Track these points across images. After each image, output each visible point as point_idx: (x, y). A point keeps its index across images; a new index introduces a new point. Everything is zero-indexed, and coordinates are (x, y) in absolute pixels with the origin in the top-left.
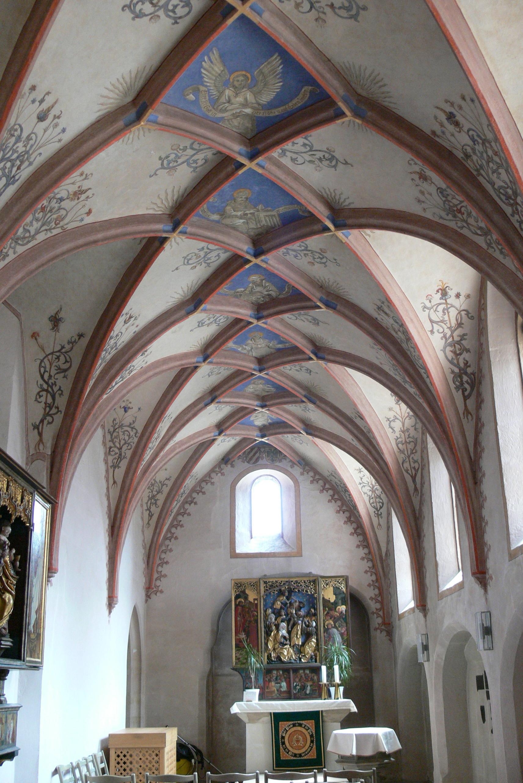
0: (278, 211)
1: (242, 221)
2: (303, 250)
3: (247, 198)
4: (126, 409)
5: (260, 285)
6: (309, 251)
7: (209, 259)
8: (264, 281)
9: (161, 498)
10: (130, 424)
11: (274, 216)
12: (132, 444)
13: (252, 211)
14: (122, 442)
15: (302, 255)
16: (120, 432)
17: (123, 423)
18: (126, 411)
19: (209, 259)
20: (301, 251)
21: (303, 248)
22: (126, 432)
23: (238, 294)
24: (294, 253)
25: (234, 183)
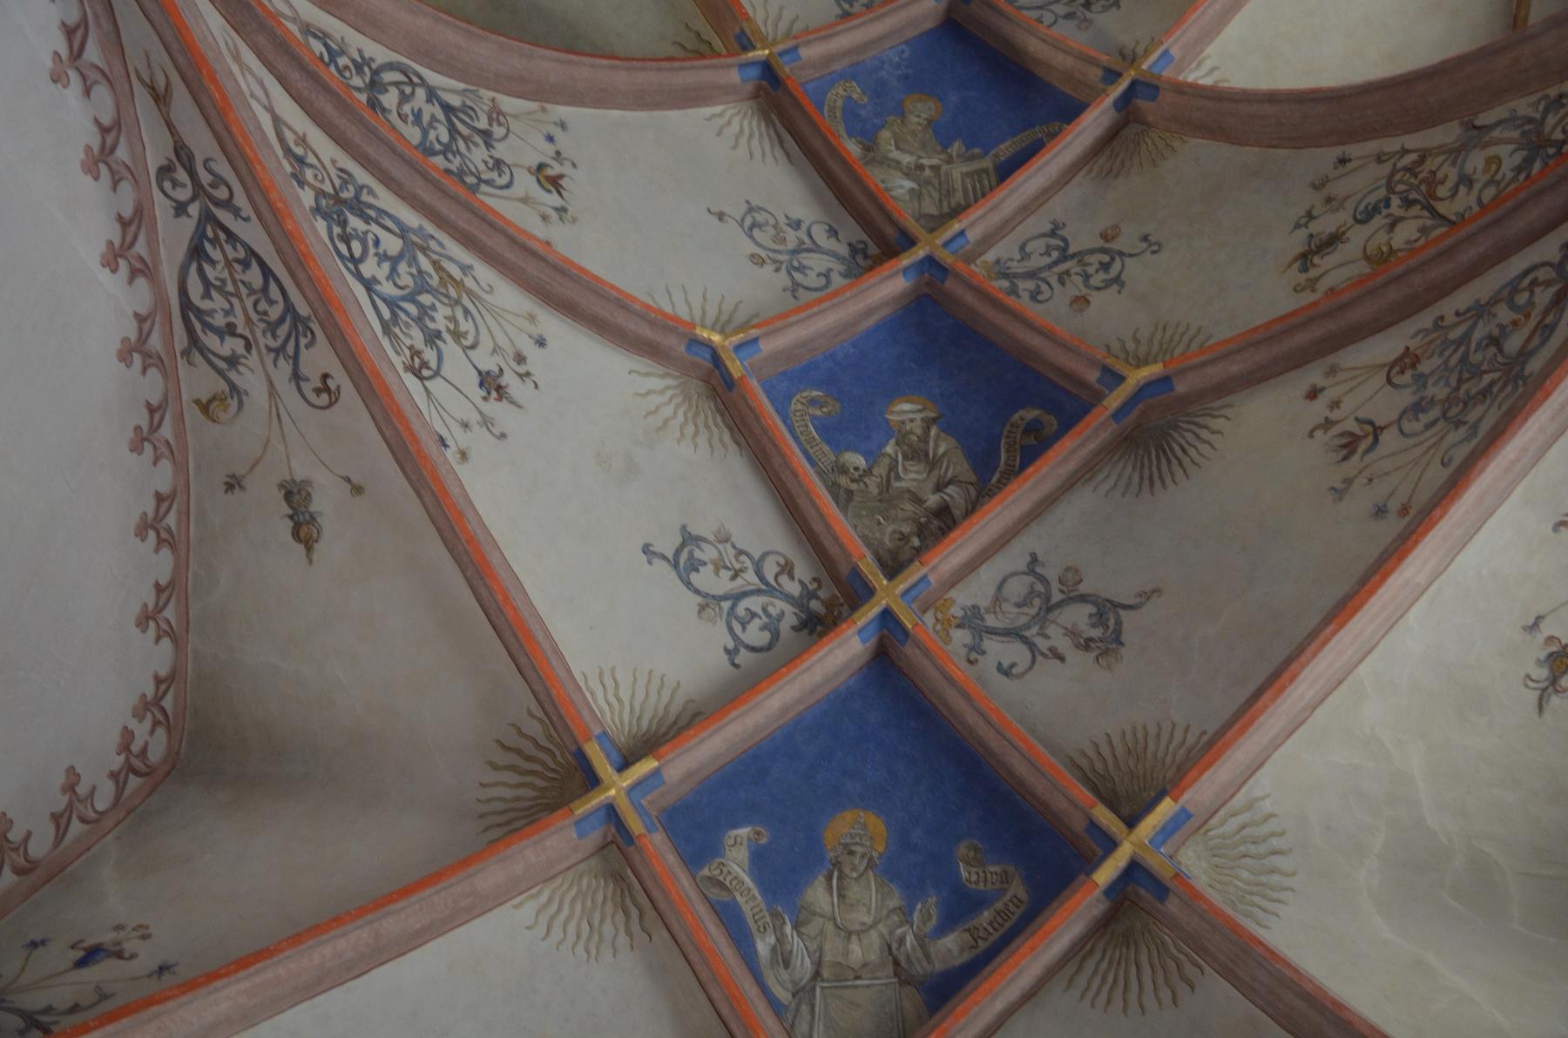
0: (996, 156)
1: (908, 184)
2: (1056, 263)
3: (930, 121)
5: (916, 453)
6: (1073, 256)
7: (801, 269)
8: (934, 431)
11: (985, 171)
13: (935, 161)
15: (1054, 281)
19: (801, 269)
20: (1050, 267)
21: (1055, 254)
23: (843, 481)
24: (1030, 285)
25: (910, 71)
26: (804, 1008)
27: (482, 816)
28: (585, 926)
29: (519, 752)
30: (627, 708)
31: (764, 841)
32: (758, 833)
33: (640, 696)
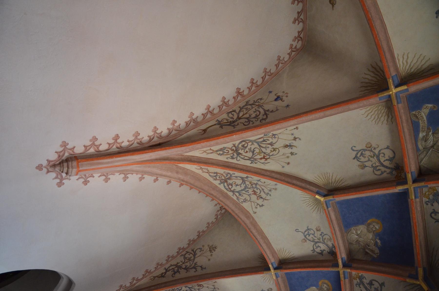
4: (278, 98)
9: (183, 274)
10: (268, 110)
12: (251, 123)
14: (247, 116)
16: (254, 109)
17: (264, 105)
18: (276, 100)
22: (258, 113)
26: (425, 152)
27: (362, 82)
28: (377, 117)
29: (375, 69)
30: (409, 65)
31: (435, 109)
32: (434, 107)
33: (415, 61)
